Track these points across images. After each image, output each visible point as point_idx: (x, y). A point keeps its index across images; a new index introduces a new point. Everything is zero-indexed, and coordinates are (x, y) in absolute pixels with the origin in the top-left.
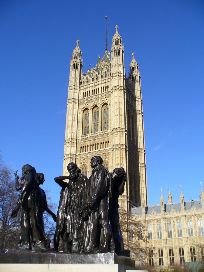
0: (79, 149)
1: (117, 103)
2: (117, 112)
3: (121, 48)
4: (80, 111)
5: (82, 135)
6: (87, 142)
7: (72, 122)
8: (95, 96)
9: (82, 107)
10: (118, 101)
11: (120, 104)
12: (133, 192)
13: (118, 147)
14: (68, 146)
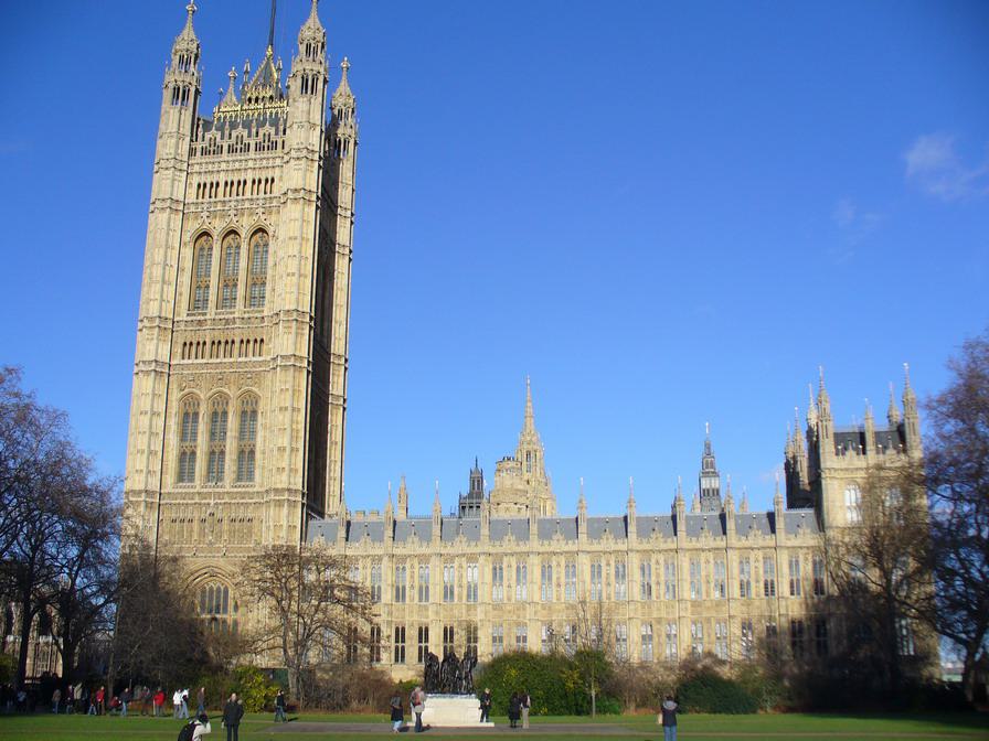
1: (296, 238)
2: (293, 268)
3: (322, 70)
6: (201, 333)
7: (164, 269)
9: (193, 226)
10: (297, 234)
11: (304, 242)
13: (287, 363)
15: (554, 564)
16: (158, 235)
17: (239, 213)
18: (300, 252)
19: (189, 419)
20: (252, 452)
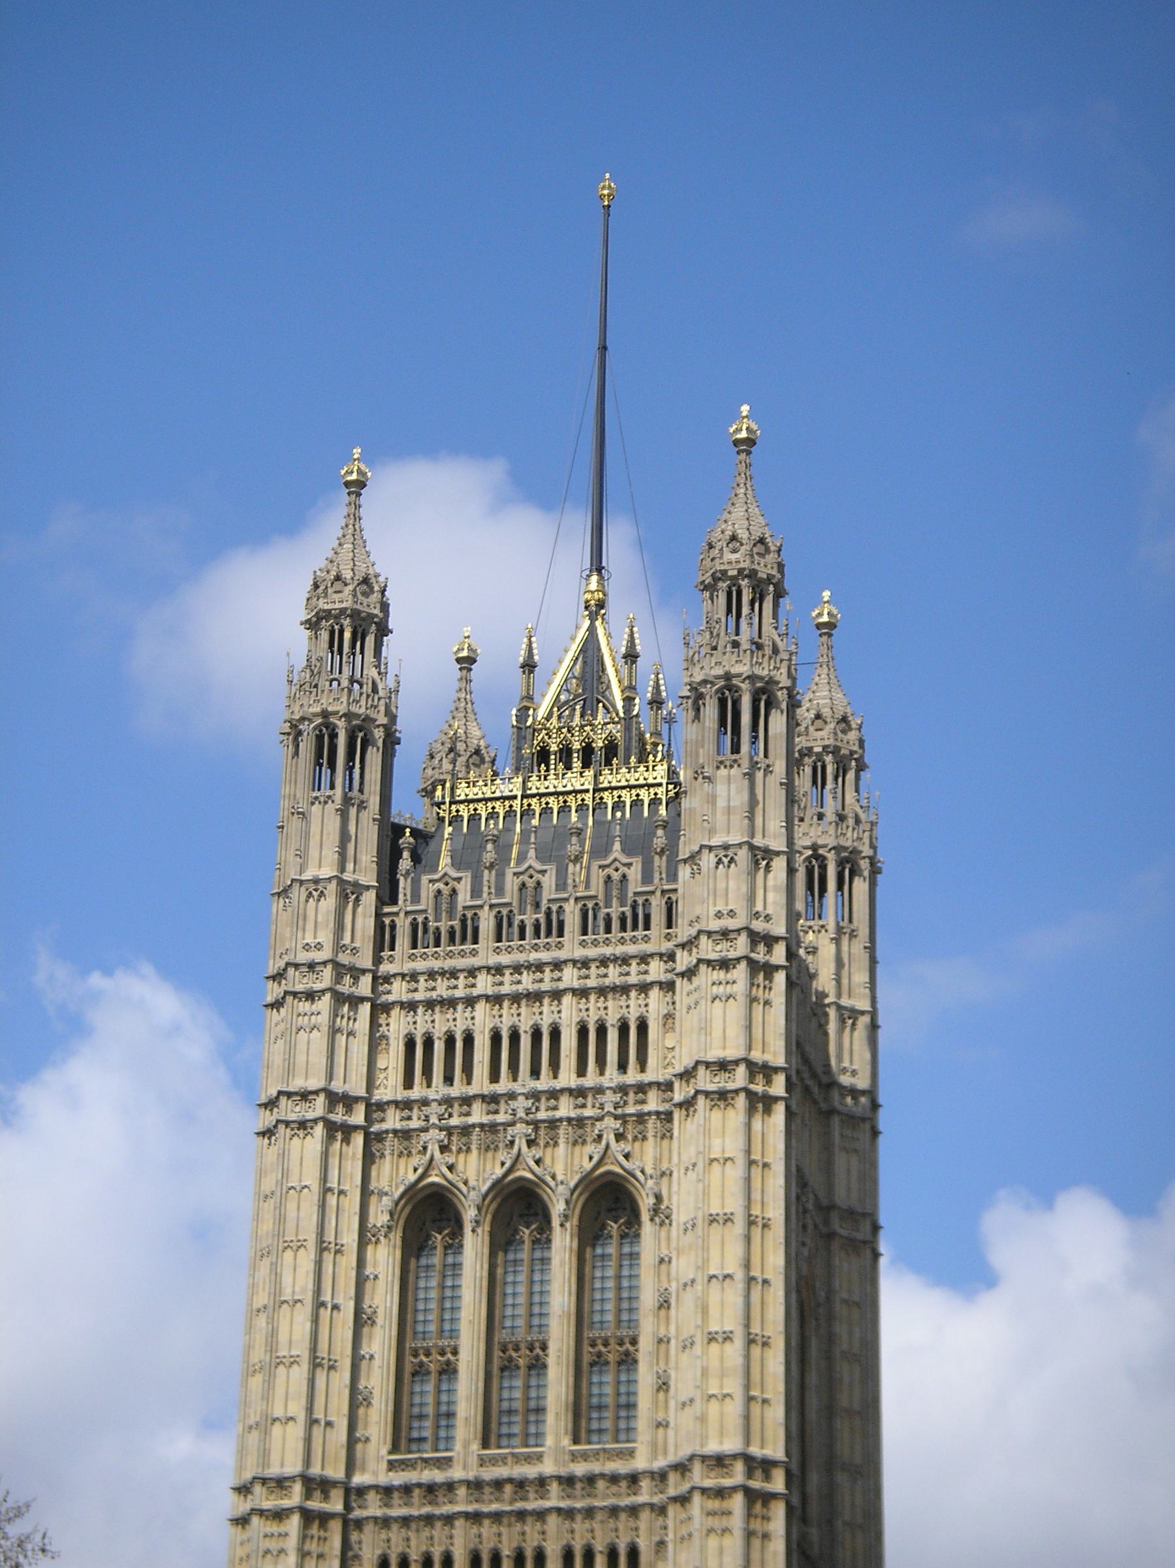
5: (395, 1449)
6: (438, 1530)
8: (521, 1104)
10: (734, 1205)
14: (273, 1545)
16: (291, 1206)
18: (747, 1265)
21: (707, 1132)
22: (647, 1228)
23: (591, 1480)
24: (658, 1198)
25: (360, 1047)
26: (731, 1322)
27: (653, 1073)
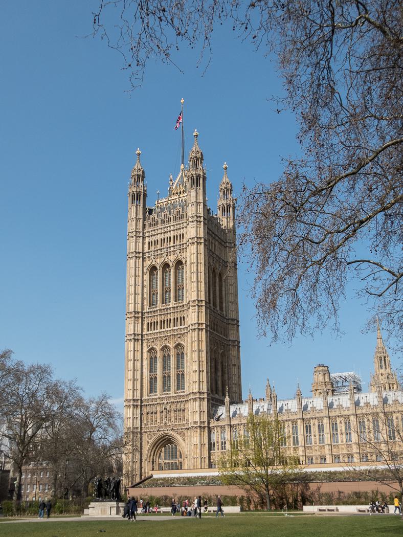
0: (145, 326)
4: (145, 271)
9: (147, 263)
11: (199, 264)
12: (220, 383)
14: (131, 322)
15: (338, 422)
17: (168, 253)
18: (197, 270)
19: (153, 361)
20: (183, 374)
21: (191, 249)
22: (184, 266)
23: (177, 307)
24: (186, 261)
25: (141, 244)
26: (195, 280)
27: (184, 242)
